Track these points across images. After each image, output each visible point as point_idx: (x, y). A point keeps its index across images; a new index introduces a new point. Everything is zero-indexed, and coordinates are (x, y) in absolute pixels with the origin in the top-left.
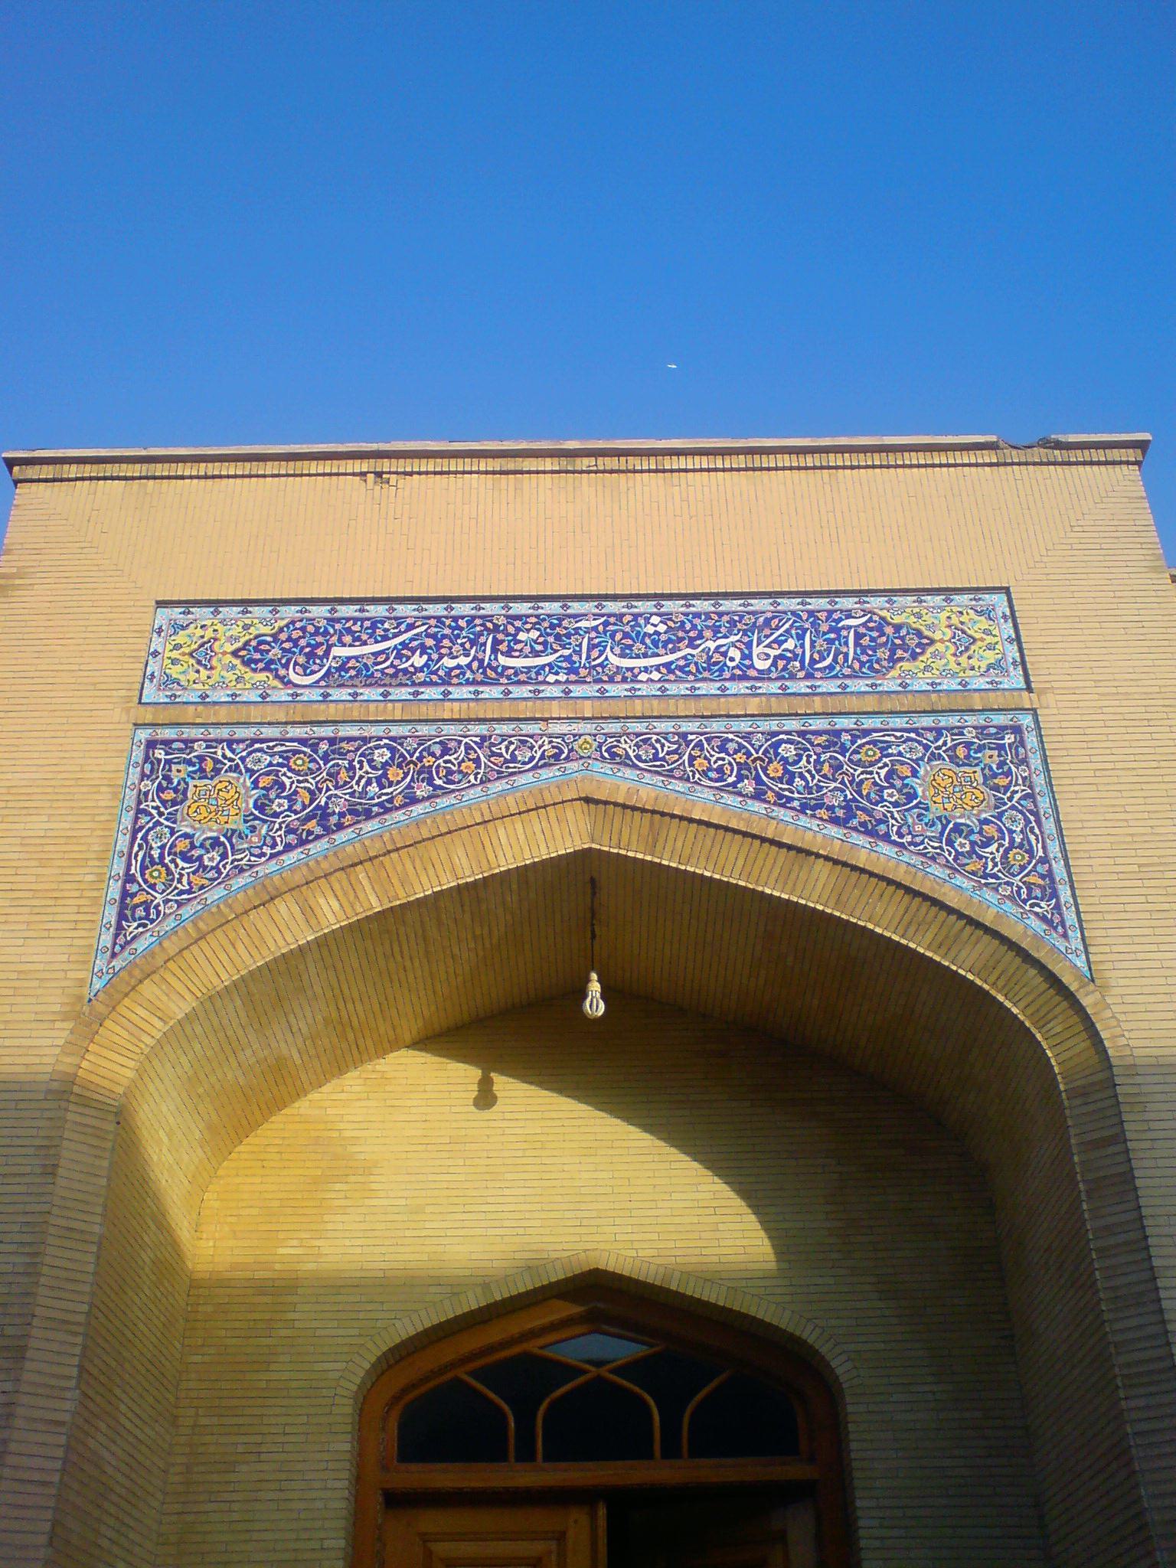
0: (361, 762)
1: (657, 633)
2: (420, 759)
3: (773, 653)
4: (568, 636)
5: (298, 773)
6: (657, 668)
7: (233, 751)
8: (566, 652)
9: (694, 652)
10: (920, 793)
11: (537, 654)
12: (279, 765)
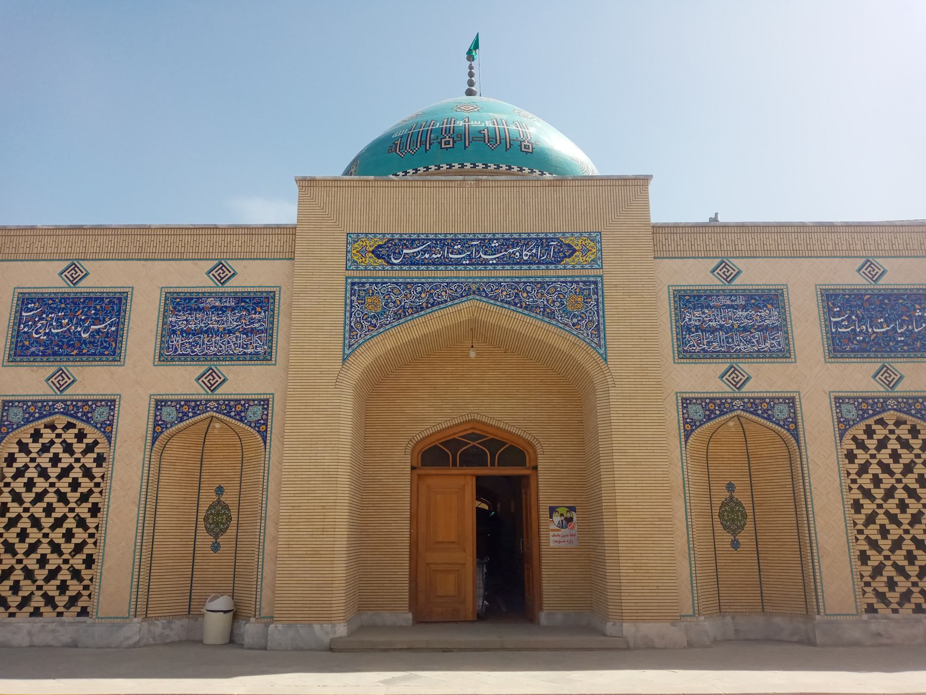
1: (495, 246)
2: (430, 290)
3: (529, 254)
4: (469, 247)
5: (395, 294)
6: (495, 258)
8: (469, 253)
9: (506, 253)
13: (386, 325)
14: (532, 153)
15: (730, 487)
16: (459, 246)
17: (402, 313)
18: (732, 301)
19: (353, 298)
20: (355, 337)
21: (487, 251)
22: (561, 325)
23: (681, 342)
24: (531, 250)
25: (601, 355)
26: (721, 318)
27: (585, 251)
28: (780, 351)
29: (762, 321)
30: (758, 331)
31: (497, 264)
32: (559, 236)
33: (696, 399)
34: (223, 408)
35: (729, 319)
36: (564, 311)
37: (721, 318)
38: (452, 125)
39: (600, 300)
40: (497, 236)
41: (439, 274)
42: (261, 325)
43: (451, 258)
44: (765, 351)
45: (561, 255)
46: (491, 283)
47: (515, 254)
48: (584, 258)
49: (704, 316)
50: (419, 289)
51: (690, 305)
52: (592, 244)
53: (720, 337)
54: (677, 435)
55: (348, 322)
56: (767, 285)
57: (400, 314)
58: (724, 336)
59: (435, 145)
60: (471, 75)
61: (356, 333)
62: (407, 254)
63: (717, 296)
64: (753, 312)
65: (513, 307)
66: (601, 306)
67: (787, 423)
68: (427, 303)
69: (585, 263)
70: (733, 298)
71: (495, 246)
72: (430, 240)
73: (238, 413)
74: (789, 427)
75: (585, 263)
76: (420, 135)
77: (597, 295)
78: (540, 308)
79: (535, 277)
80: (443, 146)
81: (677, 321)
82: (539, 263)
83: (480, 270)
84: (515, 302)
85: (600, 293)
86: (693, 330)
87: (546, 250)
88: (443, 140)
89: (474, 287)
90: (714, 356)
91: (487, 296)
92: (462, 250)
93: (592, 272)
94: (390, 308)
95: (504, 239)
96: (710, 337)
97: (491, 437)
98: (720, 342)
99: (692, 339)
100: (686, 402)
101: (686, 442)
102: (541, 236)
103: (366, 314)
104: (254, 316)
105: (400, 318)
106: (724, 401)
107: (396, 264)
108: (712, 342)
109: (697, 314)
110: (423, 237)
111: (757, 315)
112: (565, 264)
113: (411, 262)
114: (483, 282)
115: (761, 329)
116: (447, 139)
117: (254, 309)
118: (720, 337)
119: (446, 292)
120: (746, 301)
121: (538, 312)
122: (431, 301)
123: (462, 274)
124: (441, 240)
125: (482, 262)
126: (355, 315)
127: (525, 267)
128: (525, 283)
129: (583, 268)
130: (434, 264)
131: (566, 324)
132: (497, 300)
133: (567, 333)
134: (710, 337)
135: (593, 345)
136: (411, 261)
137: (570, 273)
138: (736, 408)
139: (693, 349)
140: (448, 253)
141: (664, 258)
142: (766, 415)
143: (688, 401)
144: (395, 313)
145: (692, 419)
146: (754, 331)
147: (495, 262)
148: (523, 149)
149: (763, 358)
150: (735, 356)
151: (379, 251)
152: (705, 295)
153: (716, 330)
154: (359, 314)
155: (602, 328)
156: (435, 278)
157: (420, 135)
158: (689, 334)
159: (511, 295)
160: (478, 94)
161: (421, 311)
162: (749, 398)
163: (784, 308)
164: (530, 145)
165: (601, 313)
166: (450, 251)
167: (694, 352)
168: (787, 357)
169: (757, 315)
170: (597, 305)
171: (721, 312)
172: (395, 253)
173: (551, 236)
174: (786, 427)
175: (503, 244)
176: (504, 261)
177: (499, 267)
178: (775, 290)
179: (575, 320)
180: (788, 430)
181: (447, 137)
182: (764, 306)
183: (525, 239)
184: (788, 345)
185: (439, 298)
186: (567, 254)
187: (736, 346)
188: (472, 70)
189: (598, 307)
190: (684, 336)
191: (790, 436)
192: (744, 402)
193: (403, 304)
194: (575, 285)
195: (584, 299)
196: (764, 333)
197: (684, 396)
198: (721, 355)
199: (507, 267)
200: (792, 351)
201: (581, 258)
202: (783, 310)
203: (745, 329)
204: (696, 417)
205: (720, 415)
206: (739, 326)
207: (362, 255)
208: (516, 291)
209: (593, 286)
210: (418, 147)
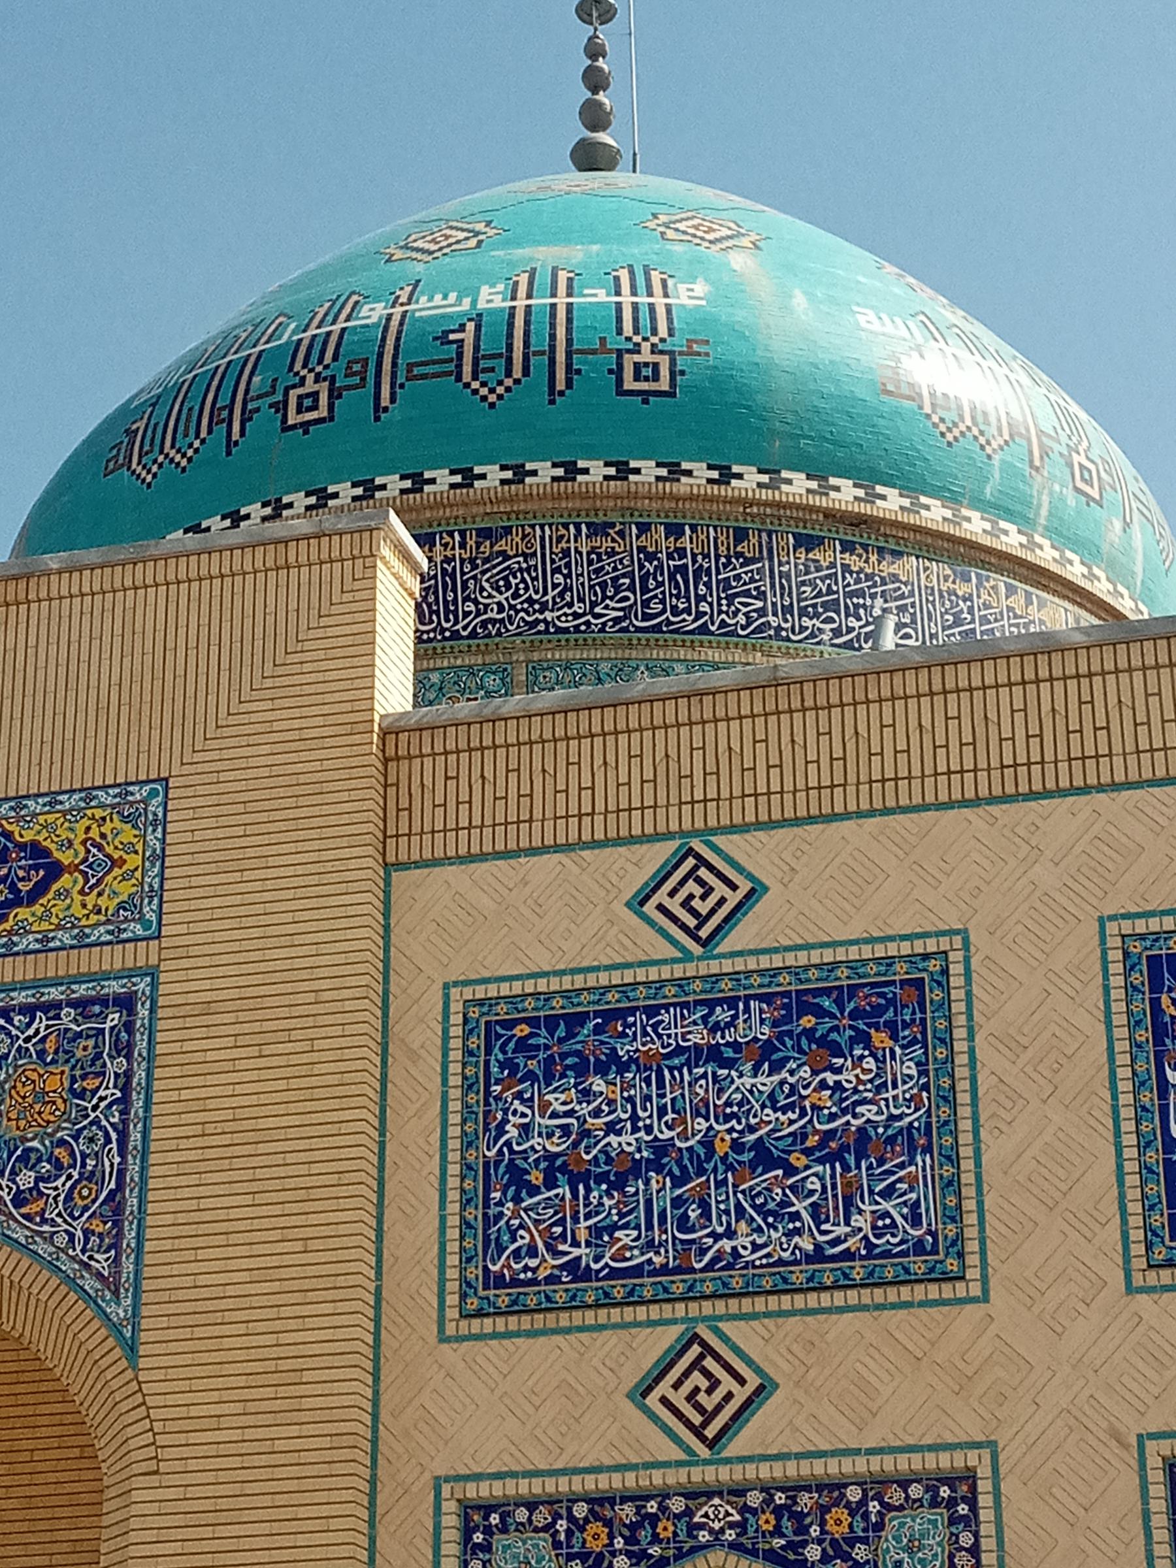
14: (671, 394)
18: (715, 1029)
25: (115, 1328)
26: (662, 1112)
28: (919, 1247)
29: (844, 1112)
30: (821, 1161)
33: (531, 1506)
37: (662, 1112)
39: (140, 1075)
44: (848, 1255)
48: (90, 900)
49: (584, 1109)
51: (532, 1064)
52: (128, 834)
53: (649, 1203)
56: (871, 940)
63: (652, 1011)
64: (805, 1072)
66: (138, 1104)
69: (94, 918)
75: (94, 918)
77: (129, 1057)
81: (468, 1143)
85: (141, 1045)
86: (536, 1177)
90: (618, 1293)
93: (115, 958)
98: (649, 1227)
106: (652, 1507)
108: (615, 1227)
109: (556, 1102)
111: (823, 1085)
118: (649, 1203)
120: (775, 1024)
129: (82, 943)
135: (90, 1284)
138: (704, 1536)
139: (526, 1268)
141: (434, 862)
146: (804, 1160)
149: (835, 1287)
150: (709, 1287)
152: (597, 1014)
153: (636, 1169)
158: (517, 1200)
163: (946, 1041)
164: (664, 362)
165: (135, 1136)
167: (534, 1282)
168: (947, 1278)
169: (823, 1085)
170: (125, 1101)
171: (661, 1084)
178: (910, 959)
179: (26, 1179)
184: (955, 1216)
187: (716, 1237)
190: (492, 1212)
192: (744, 1509)
195: (73, 1080)
196: (846, 1168)
197: (471, 1491)
198: (647, 1286)
200: (972, 1246)
201: (78, 898)
202: (941, 1053)
203: (764, 1157)
206: (737, 1146)
209: (114, 1018)
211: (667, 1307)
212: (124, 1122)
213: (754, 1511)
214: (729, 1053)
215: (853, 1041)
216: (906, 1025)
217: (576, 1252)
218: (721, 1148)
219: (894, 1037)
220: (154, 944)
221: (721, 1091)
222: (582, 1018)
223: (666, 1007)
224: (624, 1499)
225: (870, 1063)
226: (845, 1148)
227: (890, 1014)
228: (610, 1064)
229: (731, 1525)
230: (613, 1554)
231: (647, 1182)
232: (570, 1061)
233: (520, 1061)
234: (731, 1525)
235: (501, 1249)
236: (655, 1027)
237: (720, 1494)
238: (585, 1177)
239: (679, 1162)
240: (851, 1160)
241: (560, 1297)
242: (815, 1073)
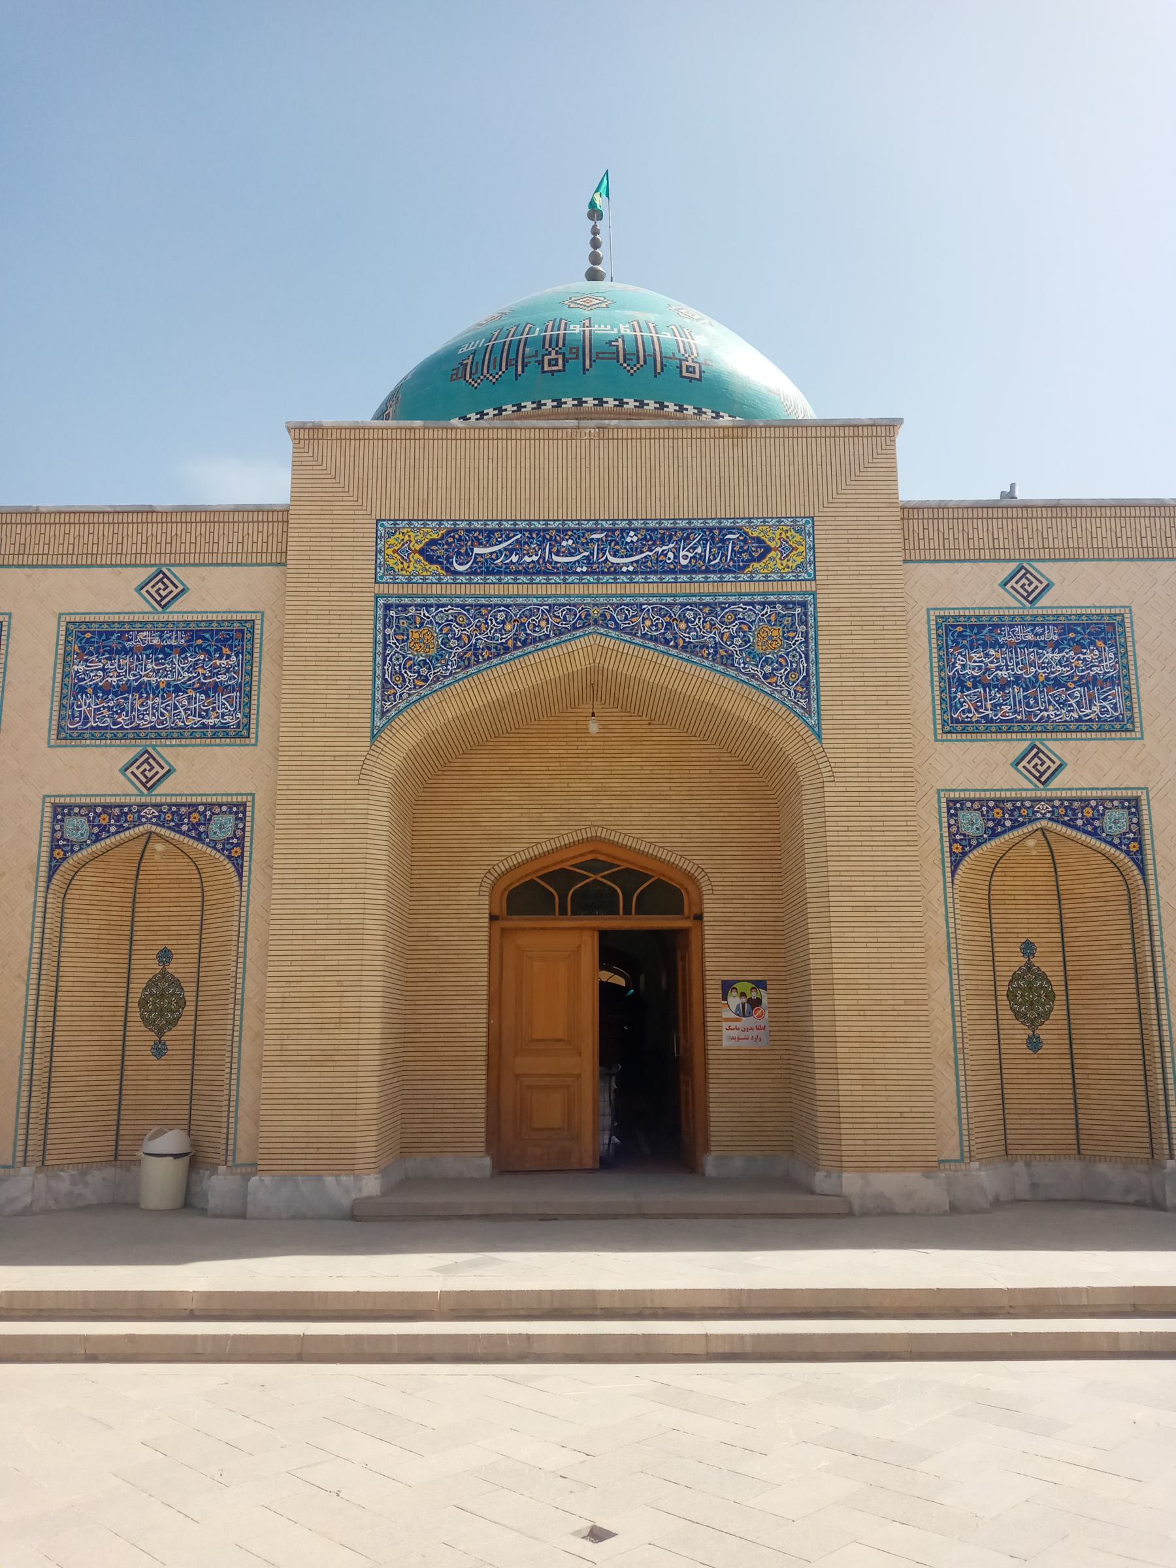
0: (491, 620)
2: (520, 618)
3: (690, 555)
4: (587, 543)
6: (632, 563)
7: (428, 612)
8: (586, 554)
10: (752, 639)
11: (571, 555)
12: (451, 620)
13: (445, 677)
14: (700, 380)
15: (1028, 948)
16: (570, 542)
17: (471, 658)
18: (1036, 635)
19: (388, 631)
20: (392, 698)
21: (618, 551)
22: (744, 678)
23: (949, 704)
24: (694, 548)
25: (812, 728)
26: (1017, 664)
27: (787, 550)
28: (1117, 719)
29: (1088, 669)
31: (635, 573)
32: (741, 523)
33: (972, 801)
34: (169, 817)
35: (1031, 665)
36: (750, 653)
37: (1017, 664)
38: (562, 332)
39: (812, 633)
40: (636, 524)
41: (536, 590)
42: (231, 678)
43: (556, 563)
44: (1091, 720)
45: (745, 556)
46: (625, 605)
47: (666, 555)
48: (785, 562)
49: (987, 660)
50: (501, 616)
53: (1014, 697)
54: (938, 862)
55: (379, 672)
56: (1095, 607)
57: (469, 660)
58: (1022, 694)
59: (533, 366)
60: (595, 244)
61: (393, 691)
62: (481, 555)
63: (1011, 626)
64: (1072, 653)
65: (661, 647)
66: (812, 644)
67: (1126, 841)
68: (515, 639)
69: (786, 570)
70: (1039, 630)
71: (632, 542)
72: (520, 531)
73: (194, 827)
74: (1128, 847)
75: (786, 570)
76: (506, 348)
78: (708, 648)
79: (700, 595)
80: (546, 369)
81: (941, 670)
82: (707, 571)
83: (606, 583)
84: (665, 639)
85: (811, 621)
86: (969, 684)
87: (720, 548)
88: (546, 358)
89: (595, 612)
90: (1004, 728)
91: (617, 628)
92: (575, 549)
94: (451, 648)
95: (647, 530)
96: (998, 695)
97: (624, 866)
98: (1015, 705)
99: (966, 700)
100: (955, 806)
101: (953, 873)
102: (712, 524)
103: (410, 659)
104: (218, 662)
105: (468, 666)
106: (1019, 804)
107: (461, 573)
108: (1001, 705)
109: (975, 657)
110: (507, 525)
111: (1079, 659)
112: (751, 572)
113: (486, 568)
114: (612, 605)
115: (1084, 682)
116: (553, 355)
117: (219, 650)
118: (1014, 697)
119: (547, 620)
120: (1060, 635)
121: (705, 655)
122: (523, 636)
123: (576, 589)
124: (539, 531)
125: (609, 569)
126: (391, 660)
127: (683, 578)
128: (683, 605)
129: (782, 579)
130: (526, 573)
131: (753, 676)
132: (635, 635)
133: (754, 691)
134: (998, 695)
135: (798, 710)
136: (487, 568)
137: (760, 588)
138: (1039, 815)
139: (967, 717)
140: (550, 553)
142: (1089, 828)
143: (958, 805)
144: (461, 657)
145: (964, 835)
146: (1073, 686)
147: (631, 568)
148: (685, 374)
150: (1039, 729)
151: (432, 550)
152: (990, 625)
153: (1008, 684)
154: (398, 659)
155: (813, 681)
156: (527, 596)
157: (506, 348)
158: (962, 692)
159: (660, 626)
160: (608, 277)
161: (504, 654)
162: (1062, 800)
163: (1124, 646)
164: (697, 366)
165: (812, 656)
166: (555, 549)
168: (1127, 730)
169: (1079, 659)
170: (806, 642)
172: (459, 554)
173: (728, 524)
174: (1124, 848)
175: (645, 539)
176: (647, 567)
177: (639, 578)
178: (1110, 615)
179: (768, 669)
180: (1128, 853)
181: (553, 352)
182: (1090, 644)
183: (683, 529)
184: (1130, 709)
185: (535, 631)
186: (756, 555)
187: (1041, 711)
188: (598, 236)
189: (807, 647)
190: (953, 695)
191: (1131, 863)
192: (1053, 807)
193: (474, 641)
194: (768, 609)
195: (784, 633)
196: (1089, 689)
197: (952, 795)
199: (653, 578)
200: (1137, 720)
201: (779, 561)
202: (1123, 650)
203: (1057, 683)
204: (971, 831)
205: (1012, 828)
206: (1047, 678)
207: (403, 558)
208: (667, 619)
209: (799, 610)
210: (504, 369)
211: (1024, 734)
212: (807, 651)
213: (1057, 807)
214: (1042, 644)
215: (1090, 644)
216: (1109, 639)
217: (987, 712)
218: (1041, 679)
219: (1105, 643)
220: (813, 582)
221: (1040, 658)
222: (984, 626)
223: (1017, 625)
224: (1008, 801)
225: (1096, 652)
226: (1088, 682)
227: (1103, 635)
228: (996, 645)
229: (1049, 812)
230: (1005, 819)
231: (1013, 689)
232: (980, 642)
233: (960, 640)
234: (1049, 812)
235: (957, 710)
236: (1013, 632)
237: (1044, 801)
238: (989, 685)
239: (1025, 682)
240: (1091, 687)
241: (982, 728)
242: (1075, 654)
